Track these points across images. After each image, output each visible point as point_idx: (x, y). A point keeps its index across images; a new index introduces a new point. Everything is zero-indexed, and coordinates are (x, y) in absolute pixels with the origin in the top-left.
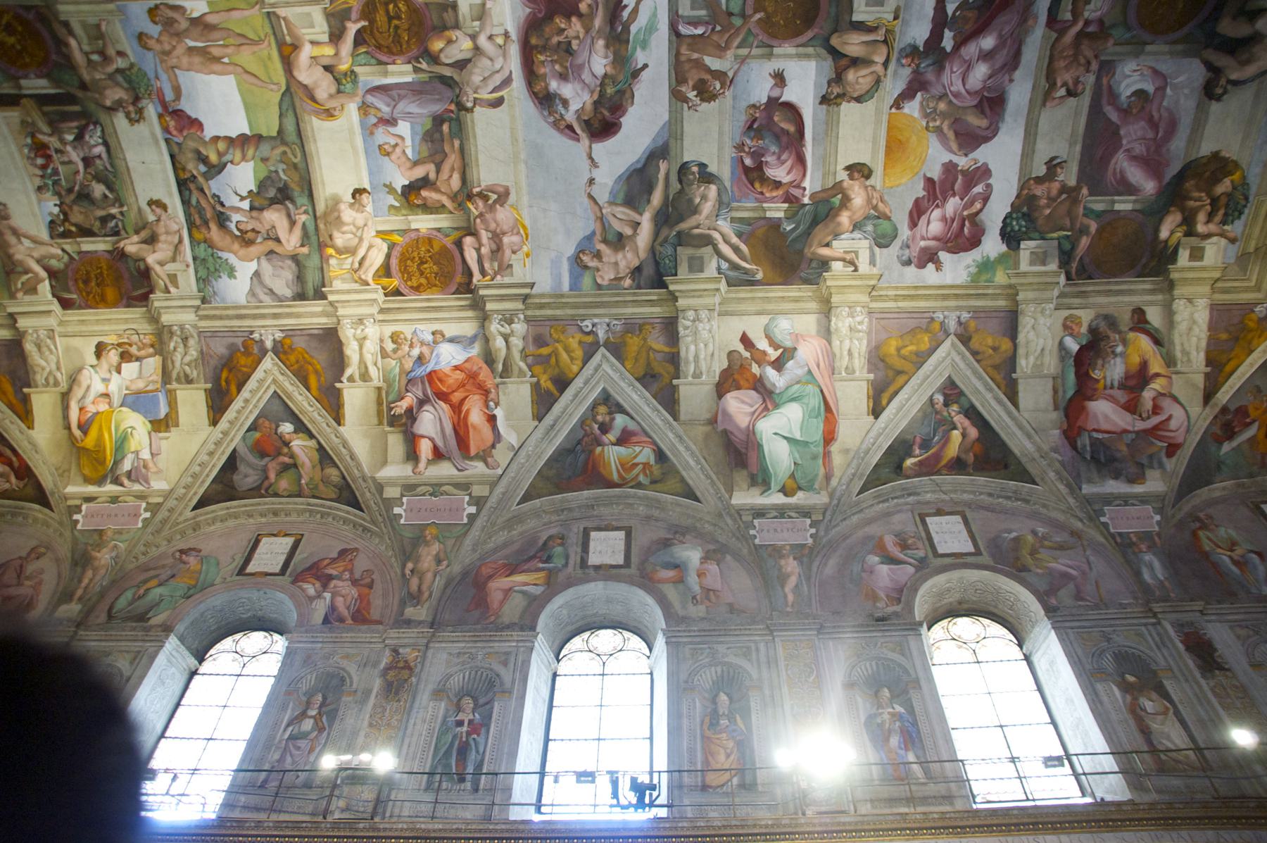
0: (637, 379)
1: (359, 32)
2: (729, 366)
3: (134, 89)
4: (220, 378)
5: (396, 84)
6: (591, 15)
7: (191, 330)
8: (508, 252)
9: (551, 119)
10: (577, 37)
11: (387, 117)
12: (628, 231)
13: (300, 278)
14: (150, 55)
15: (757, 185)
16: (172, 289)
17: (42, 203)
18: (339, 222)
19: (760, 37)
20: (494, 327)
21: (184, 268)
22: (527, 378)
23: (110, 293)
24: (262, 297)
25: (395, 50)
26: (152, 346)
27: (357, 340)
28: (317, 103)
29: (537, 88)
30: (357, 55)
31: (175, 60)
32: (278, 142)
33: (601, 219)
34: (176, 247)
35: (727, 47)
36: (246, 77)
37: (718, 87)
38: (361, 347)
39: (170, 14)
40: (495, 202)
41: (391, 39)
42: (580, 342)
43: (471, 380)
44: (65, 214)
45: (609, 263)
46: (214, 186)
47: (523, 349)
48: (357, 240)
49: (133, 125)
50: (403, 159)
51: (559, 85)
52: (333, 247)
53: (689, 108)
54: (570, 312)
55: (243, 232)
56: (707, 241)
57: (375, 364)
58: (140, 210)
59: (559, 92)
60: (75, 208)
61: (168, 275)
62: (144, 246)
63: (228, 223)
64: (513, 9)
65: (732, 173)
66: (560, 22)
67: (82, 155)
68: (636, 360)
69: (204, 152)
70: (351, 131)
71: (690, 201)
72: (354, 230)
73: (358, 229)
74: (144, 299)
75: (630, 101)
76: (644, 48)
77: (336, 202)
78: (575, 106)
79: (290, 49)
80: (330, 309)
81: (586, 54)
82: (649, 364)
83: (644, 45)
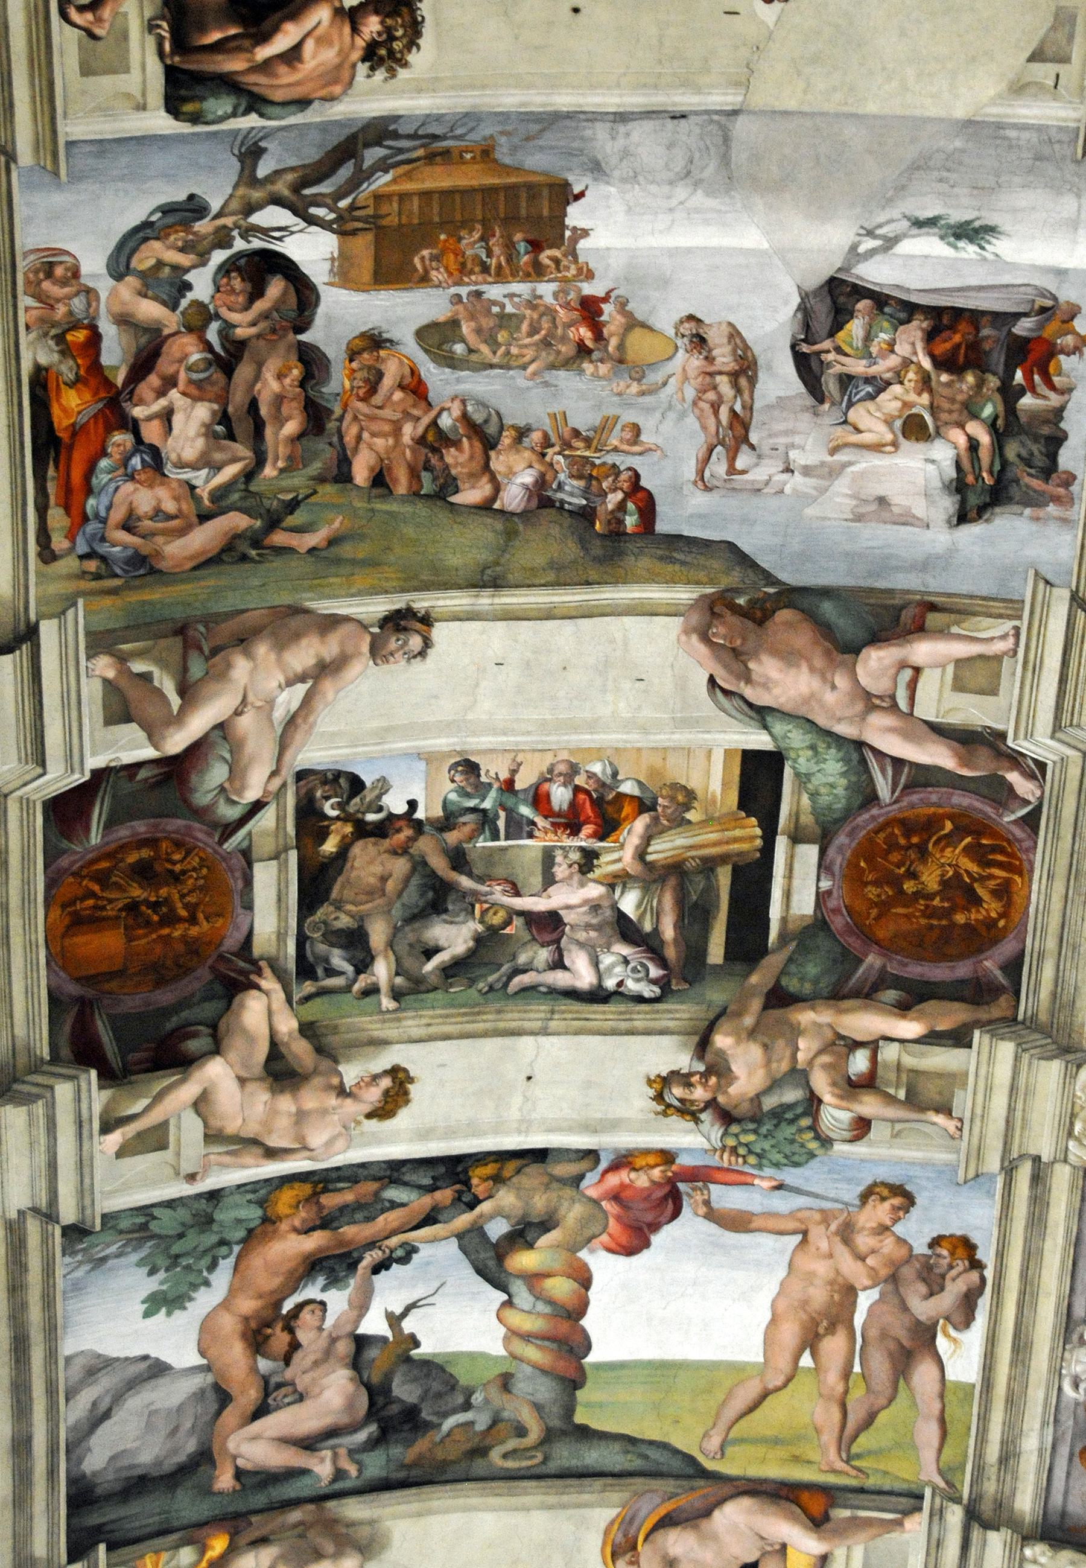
3: (753, 1119)
14: (851, 1193)
16: (115, 1138)
17: (422, 765)
31: (824, 1245)
32: (556, 1423)
34: (255, 1142)
39: (955, 1289)
44: (381, 830)
49: (650, 1082)
55: (290, 1322)
60: (400, 866)
61: (164, 1126)
62: (262, 1050)
63: (321, 1281)
67: (568, 917)
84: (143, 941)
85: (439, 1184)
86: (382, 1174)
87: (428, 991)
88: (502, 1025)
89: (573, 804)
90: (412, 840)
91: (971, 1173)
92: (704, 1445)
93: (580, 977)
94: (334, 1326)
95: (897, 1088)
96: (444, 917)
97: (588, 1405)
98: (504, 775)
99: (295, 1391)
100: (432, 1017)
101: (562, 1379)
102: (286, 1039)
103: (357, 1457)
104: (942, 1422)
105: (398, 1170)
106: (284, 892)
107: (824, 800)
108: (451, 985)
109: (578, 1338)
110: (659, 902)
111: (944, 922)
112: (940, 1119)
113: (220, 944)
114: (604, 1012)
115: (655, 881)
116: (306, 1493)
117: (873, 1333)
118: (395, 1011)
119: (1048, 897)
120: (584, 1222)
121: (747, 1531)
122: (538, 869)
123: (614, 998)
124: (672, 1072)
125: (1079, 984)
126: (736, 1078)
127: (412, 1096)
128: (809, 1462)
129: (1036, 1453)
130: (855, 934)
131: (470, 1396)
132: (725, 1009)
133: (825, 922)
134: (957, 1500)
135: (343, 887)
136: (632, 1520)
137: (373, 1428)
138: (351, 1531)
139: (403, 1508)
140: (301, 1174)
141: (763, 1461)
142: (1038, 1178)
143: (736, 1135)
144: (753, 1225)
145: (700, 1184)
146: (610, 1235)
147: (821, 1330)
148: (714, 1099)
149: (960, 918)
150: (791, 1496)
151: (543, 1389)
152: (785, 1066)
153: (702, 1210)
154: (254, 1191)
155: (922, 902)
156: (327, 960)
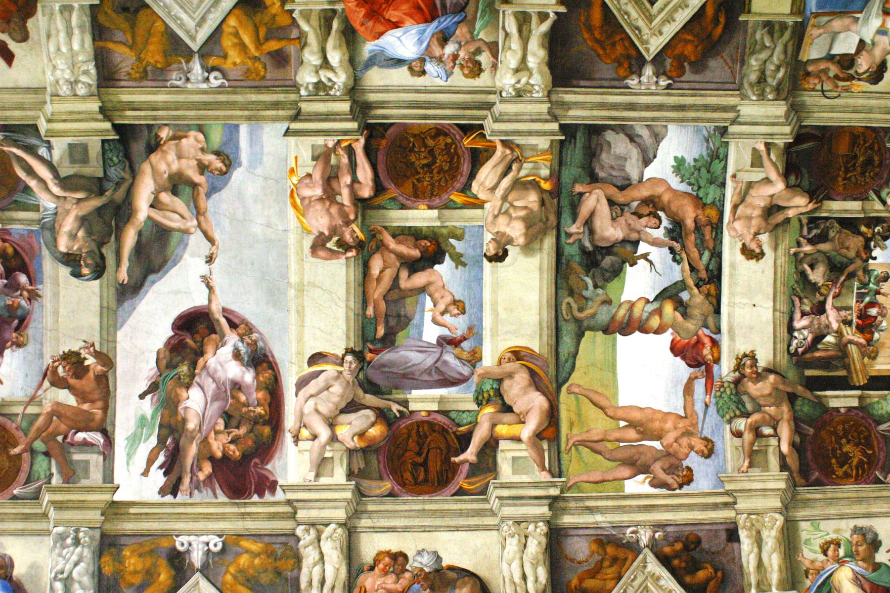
0: (147, 6)
1: (464, 449)
2: (25, 22)
3: (737, 394)
4: (726, 26)
5: (430, 387)
6: (199, 458)
7: (750, 93)
8: (317, 176)
9: (255, 336)
10: (217, 433)
11: (449, 348)
12: (166, 197)
13: (591, 154)
14: (707, 433)
15: (10, 250)
16: (761, 147)
18: (529, 222)
19: (14, 425)
20: (341, 79)
21: (740, 176)
22: (298, 8)
23: (843, 148)
24: (645, 133)
25: (426, 428)
26: (808, 74)
27: (528, 69)
28: (529, 368)
29: (268, 374)
30: (470, 423)
31: (681, 425)
32: (585, 324)
33: (199, 213)
34: (743, 200)
35: (51, 415)
36: (603, 402)
37: (60, 370)
38: (524, 59)
39: (669, 479)
40: (329, 238)
41: (428, 440)
42: (225, 57)
43: (376, 7)
44: (868, 249)
45: (188, 158)
46: (676, 273)
47: (302, 48)
48: (510, 198)
49: (752, 352)
50: (437, 295)
51: (243, 377)
52: (542, 191)
53: (93, 345)
54: (239, 98)
56: (66, 183)
57: (507, 35)
58: (776, 249)
59: (244, 369)
60: (852, 254)
61: (762, 166)
63: (670, 226)
64: (285, 468)
65: (41, 266)
66: (235, 451)
67: (823, 317)
68: (149, 33)
69: (678, 315)
70: (494, 334)
71: (89, 233)
72: (511, 211)
73: (506, 212)
74: (801, 136)
75: (162, 356)
76: (143, 418)
78: (226, 352)
79: (545, 434)
80: (558, 112)
81: (208, 413)
82: (133, 26)
83: (142, 421)
88: (778, 294)
89: (870, 316)
90: (862, 259)
97: (595, 336)
98: (882, 291)
104: (604, 481)
107: (876, 406)
112: (746, 464)
117: (641, 449)
119: (848, 492)
120: (687, 330)
121: (530, 406)
122: (844, 305)
124: (757, 360)
127: (751, 261)
128: (571, 430)
134: (562, 491)
137: (591, 249)
138: (538, 240)
139: (546, 262)
142: (726, 505)
147: (638, 428)
149: (833, 461)
152: (762, 402)
154: (719, 201)
156: (816, 227)
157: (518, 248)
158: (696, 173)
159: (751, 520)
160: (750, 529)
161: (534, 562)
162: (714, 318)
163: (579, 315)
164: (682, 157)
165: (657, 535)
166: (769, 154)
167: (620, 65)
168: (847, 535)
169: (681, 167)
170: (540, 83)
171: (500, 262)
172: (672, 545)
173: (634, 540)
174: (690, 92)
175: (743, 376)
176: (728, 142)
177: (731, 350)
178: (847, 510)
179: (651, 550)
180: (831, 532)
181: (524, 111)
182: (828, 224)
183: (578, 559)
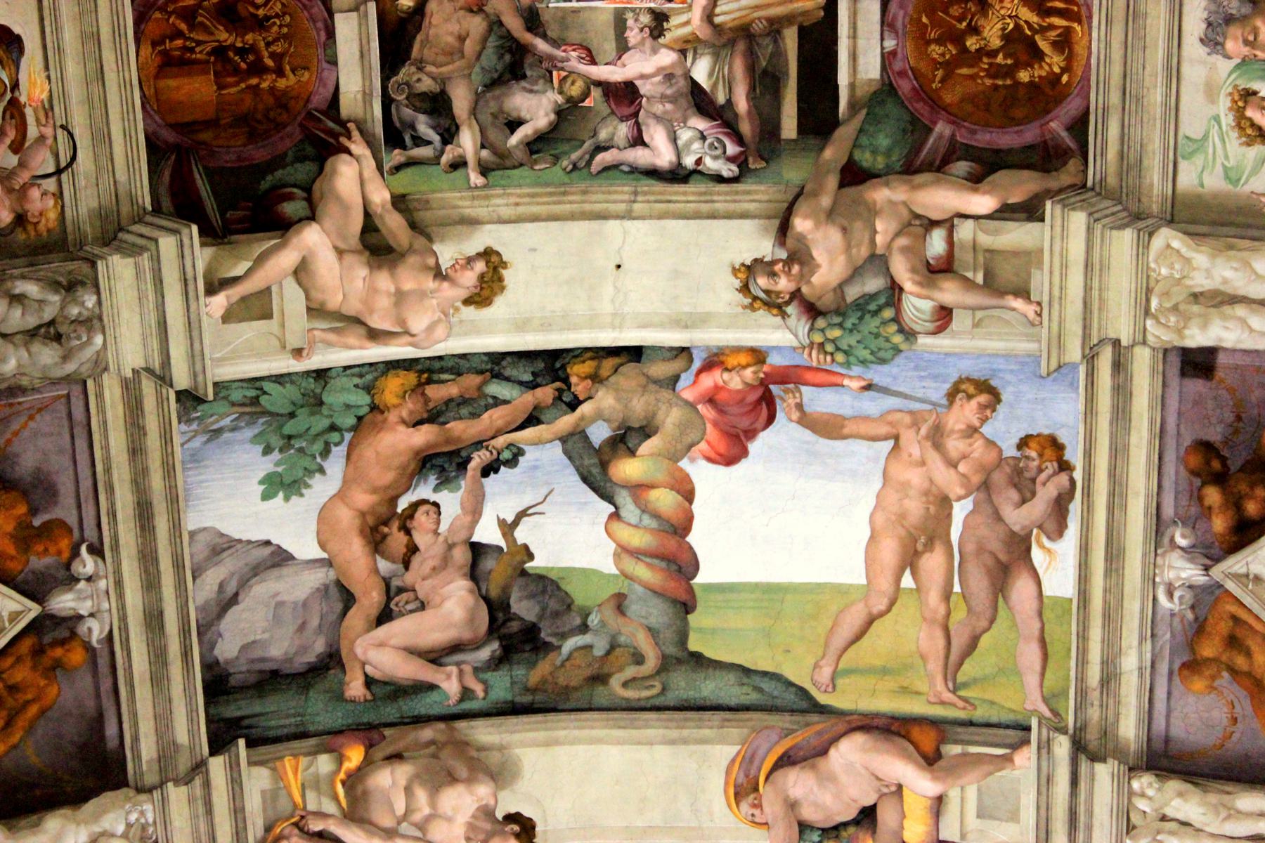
3: (838, 312)
7: (89, 353)
14: (938, 392)
16: (219, 302)
18: (440, 779)
21: (293, 341)
31: (916, 451)
32: (671, 650)
34: (357, 321)
39: (1047, 493)
48: (387, 822)
49: (735, 271)
52: (368, 763)
58: (473, 222)
60: (476, 25)
61: (267, 291)
63: (433, 480)
67: (645, 88)
69: (647, 447)
72: (417, 817)
73: (422, 827)
77: (501, 775)
80: (184, 764)
84: (233, 90)
85: (539, 380)
86: (484, 366)
87: (515, 167)
88: (587, 207)
91: (1054, 365)
92: (815, 677)
93: (659, 155)
94: (449, 530)
95: (975, 270)
96: (523, 84)
97: (700, 630)
99: (417, 598)
100: (519, 196)
101: (675, 602)
102: (379, 210)
103: (482, 676)
105: (498, 364)
106: (366, 48)
108: (536, 162)
109: (686, 556)
110: (730, 68)
111: (1009, 82)
112: (1018, 304)
113: (308, 101)
114: (685, 194)
115: (724, 46)
116: (435, 711)
117: (970, 547)
118: (485, 186)
119: (1108, 44)
120: (683, 427)
121: (863, 771)
123: (695, 176)
124: (756, 260)
125: (1145, 141)
126: (818, 266)
127: (506, 283)
128: (918, 693)
129: (1136, 673)
130: (923, 100)
131: (588, 615)
132: (803, 188)
133: (891, 84)
134: (1064, 731)
135: (423, 46)
136: (753, 756)
137: (495, 645)
138: (483, 755)
139: (531, 735)
140: (405, 360)
141: (874, 693)
142: (1119, 366)
143: (823, 330)
144: (846, 431)
145: (791, 386)
146: (708, 443)
147: (920, 547)
148: (799, 290)
149: (1024, 76)
150: (903, 733)
151: (655, 612)
152: (864, 252)
153: (796, 415)
154: (361, 376)
155: (985, 60)
156: (412, 127)
157: (502, 795)
158: (298, 444)
159: (1160, 308)
160: (1187, 318)
161: (1224, 814)
162: (652, 361)
163: (651, 663)
164: (261, 482)
165: (1182, 541)
166: (235, 280)
167: (57, 665)
168: (1224, 66)
169: (287, 480)
170: (122, 813)
171: (533, 827)
172: (1207, 512)
173: (1189, 597)
174: (102, 498)
175: (796, 295)
176: (216, 384)
177: (731, 325)
178: (1157, 55)
179: (1217, 560)
180: (1212, 110)
181: (188, 830)
182: (401, 98)
183: (1225, 722)
